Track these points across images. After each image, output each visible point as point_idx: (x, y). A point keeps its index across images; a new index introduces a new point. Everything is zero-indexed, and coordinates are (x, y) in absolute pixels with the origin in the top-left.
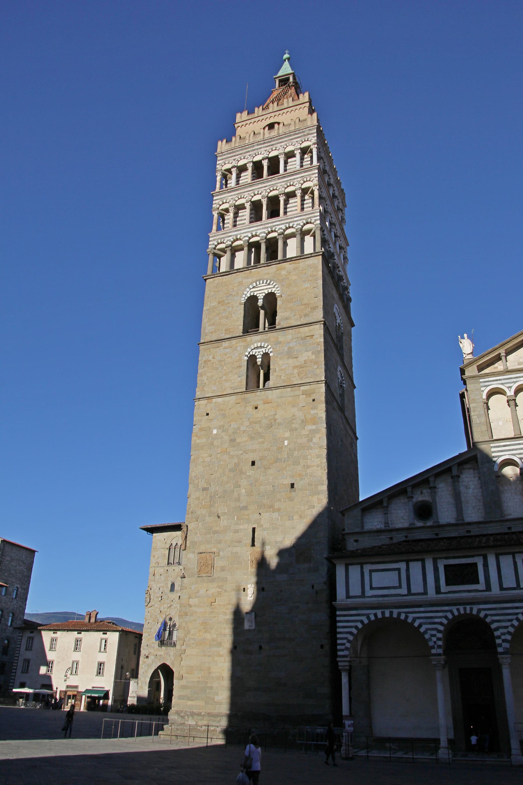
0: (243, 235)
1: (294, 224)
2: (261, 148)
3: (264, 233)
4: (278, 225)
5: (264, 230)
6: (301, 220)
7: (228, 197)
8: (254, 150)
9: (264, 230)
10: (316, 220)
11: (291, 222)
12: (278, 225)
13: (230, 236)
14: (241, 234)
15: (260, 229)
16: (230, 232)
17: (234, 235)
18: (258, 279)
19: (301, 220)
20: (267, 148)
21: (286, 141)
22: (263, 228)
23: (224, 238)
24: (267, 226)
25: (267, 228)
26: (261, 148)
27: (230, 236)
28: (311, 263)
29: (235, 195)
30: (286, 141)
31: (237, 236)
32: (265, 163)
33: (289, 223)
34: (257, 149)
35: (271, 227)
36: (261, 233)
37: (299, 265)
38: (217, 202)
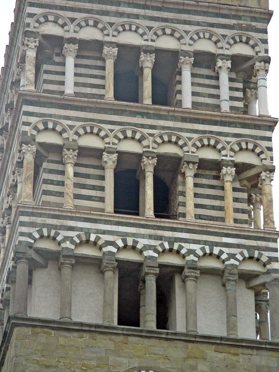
0: (105, 238)
1: (221, 252)
2: (137, 16)
3: (156, 251)
4: (186, 241)
5: (153, 242)
6: (238, 246)
7: (60, 117)
8: (122, 15)
9: (153, 242)
10: (271, 259)
11: (217, 244)
12: (186, 241)
13: (72, 229)
14: (98, 232)
15: (143, 236)
16: (72, 218)
17: (81, 229)
18: (144, 365)
19: (238, 246)
20: (155, 25)
21: (198, 24)
22: (150, 237)
23: (55, 227)
24: (160, 233)
25: (160, 238)
26: (137, 16)
27: (72, 229)
28: (263, 363)
29: (78, 119)
30: (198, 24)
31: (88, 232)
32: (148, 62)
33: (213, 244)
34: (129, 16)
35: (172, 241)
36: (147, 247)
37: (235, 358)
38: (33, 120)
